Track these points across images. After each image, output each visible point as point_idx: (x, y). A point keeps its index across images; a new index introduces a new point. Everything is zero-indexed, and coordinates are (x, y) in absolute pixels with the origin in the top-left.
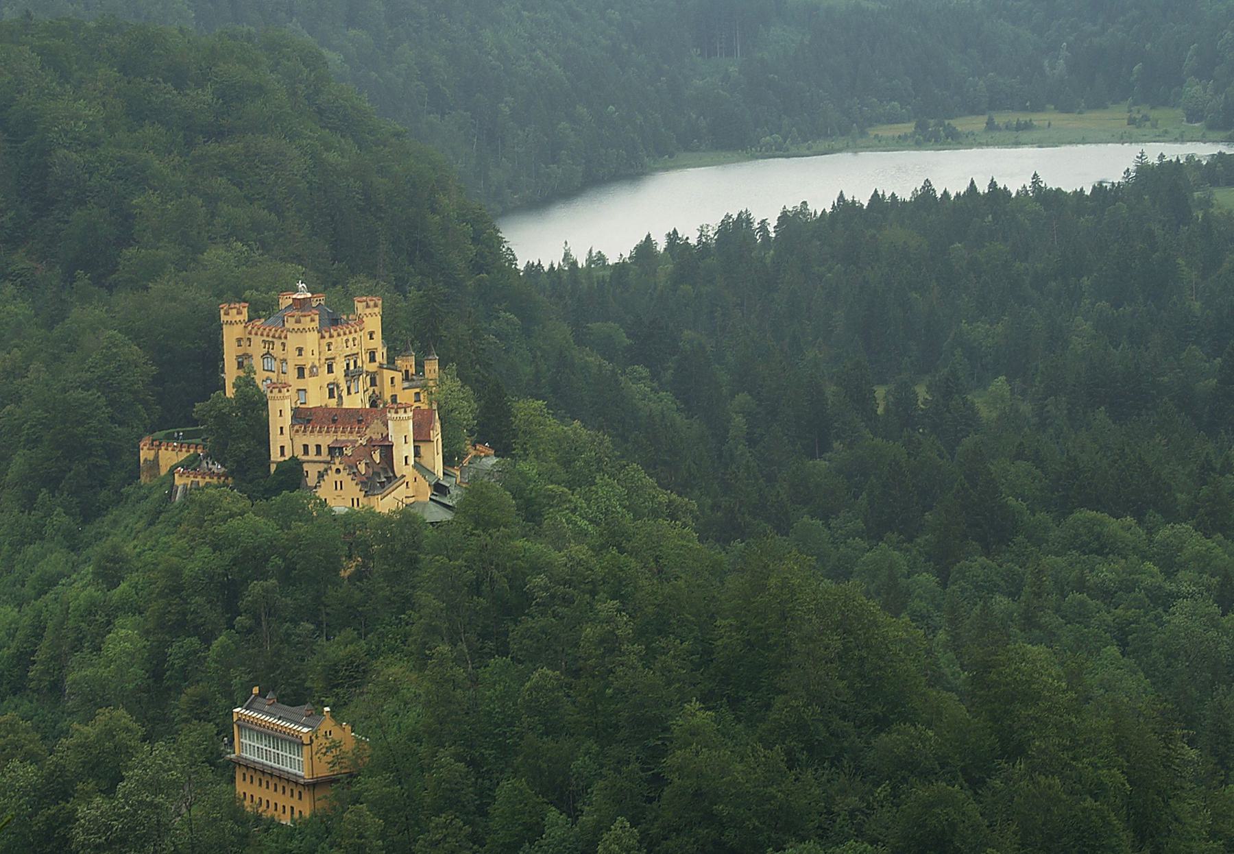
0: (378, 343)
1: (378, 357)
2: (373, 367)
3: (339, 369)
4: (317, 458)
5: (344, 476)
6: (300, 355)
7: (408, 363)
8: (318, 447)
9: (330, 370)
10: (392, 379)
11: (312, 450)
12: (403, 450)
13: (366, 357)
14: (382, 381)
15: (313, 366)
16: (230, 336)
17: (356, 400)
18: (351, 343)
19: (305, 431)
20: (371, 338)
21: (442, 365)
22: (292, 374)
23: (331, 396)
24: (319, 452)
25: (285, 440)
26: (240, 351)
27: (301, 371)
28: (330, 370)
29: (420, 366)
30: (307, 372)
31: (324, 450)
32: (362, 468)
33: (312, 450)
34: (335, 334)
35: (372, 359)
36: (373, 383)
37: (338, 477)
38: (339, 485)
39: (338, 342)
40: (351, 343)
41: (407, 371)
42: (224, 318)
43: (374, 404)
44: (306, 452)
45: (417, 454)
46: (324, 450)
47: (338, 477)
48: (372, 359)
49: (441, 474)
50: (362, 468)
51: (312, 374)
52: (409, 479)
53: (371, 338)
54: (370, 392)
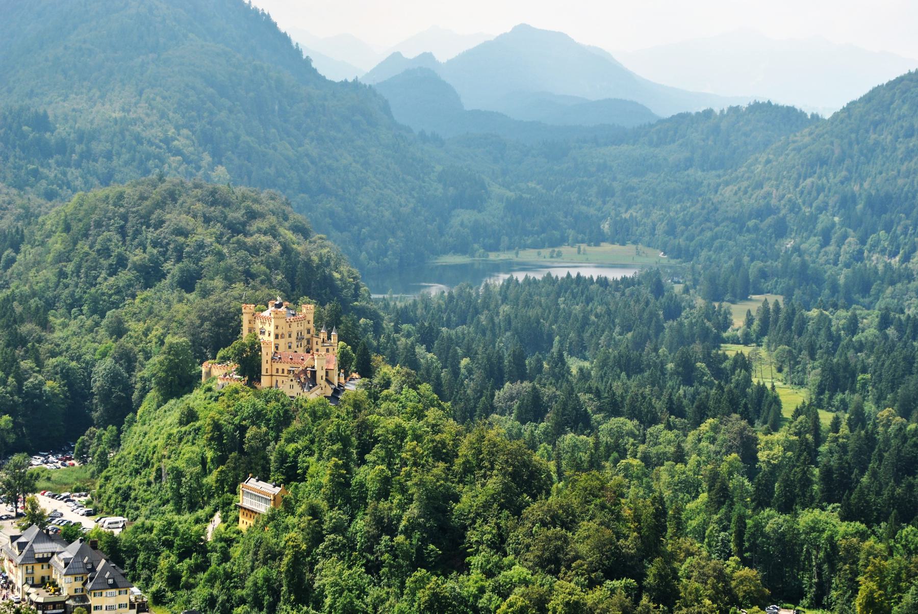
0: (311, 325)
2: (309, 336)
3: (294, 335)
5: (295, 383)
7: (323, 334)
9: (290, 336)
11: (280, 371)
13: (306, 332)
16: (245, 319)
21: (340, 339)
22: (272, 335)
25: (268, 366)
26: (250, 326)
27: (277, 337)
28: (290, 336)
29: (329, 338)
31: (286, 372)
33: (280, 371)
35: (309, 332)
36: (308, 342)
37: (292, 383)
38: (292, 387)
42: (243, 311)
45: (327, 375)
46: (286, 372)
47: (292, 383)
48: (309, 332)
51: (282, 337)
52: (323, 386)
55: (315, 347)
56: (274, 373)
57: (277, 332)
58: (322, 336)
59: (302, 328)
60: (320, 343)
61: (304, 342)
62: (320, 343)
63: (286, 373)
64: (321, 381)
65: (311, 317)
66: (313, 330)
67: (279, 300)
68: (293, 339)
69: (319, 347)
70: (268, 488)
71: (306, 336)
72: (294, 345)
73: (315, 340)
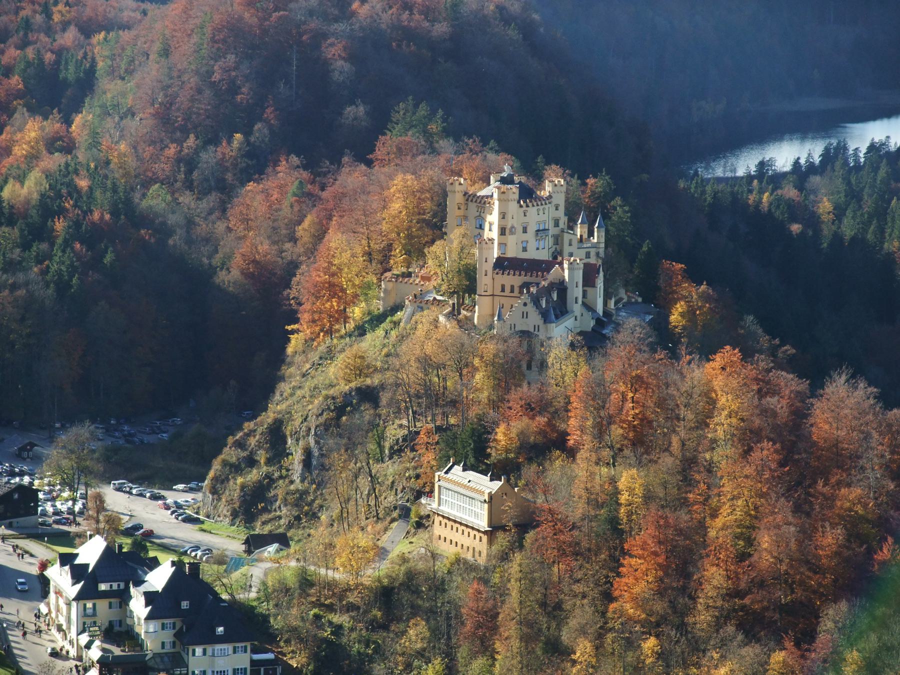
1: (561, 225)
3: (532, 229)
4: (512, 295)
5: (531, 309)
6: (503, 218)
8: (512, 287)
9: (525, 230)
10: (571, 241)
11: (508, 289)
12: (576, 292)
13: (552, 224)
14: (563, 240)
15: (513, 227)
17: (544, 255)
18: (541, 212)
19: (503, 274)
20: (557, 209)
23: (525, 249)
24: (512, 291)
28: (525, 230)
29: (591, 234)
30: (507, 231)
32: (544, 304)
33: (508, 289)
34: (530, 204)
35: (557, 224)
37: (525, 309)
39: (532, 211)
40: (541, 212)
41: (581, 236)
43: (555, 258)
44: (503, 290)
45: (584, 296)
46: (516, 290)
47: (525, 309)
48: (557, 224)
49: (601, 314)
50: (544, 304)
53: (557, 209)
54: (553, 249)
55: (567, 249)
56: (498, 291)
57: (503, 222)
58: (579, 231)
59: (545, 217)
60: (575, 243)
61: (550, 241)
62: (575, 243)
63: (516, 293)
64: (577, 309)
65: (560, 199)
66: (563, 220)
67: (507, 170)
68: (530, 236)
69: (573, 249)
70: (488, 485)
71: (553, 231)
72: (532, 245)
73: (567, 237)
